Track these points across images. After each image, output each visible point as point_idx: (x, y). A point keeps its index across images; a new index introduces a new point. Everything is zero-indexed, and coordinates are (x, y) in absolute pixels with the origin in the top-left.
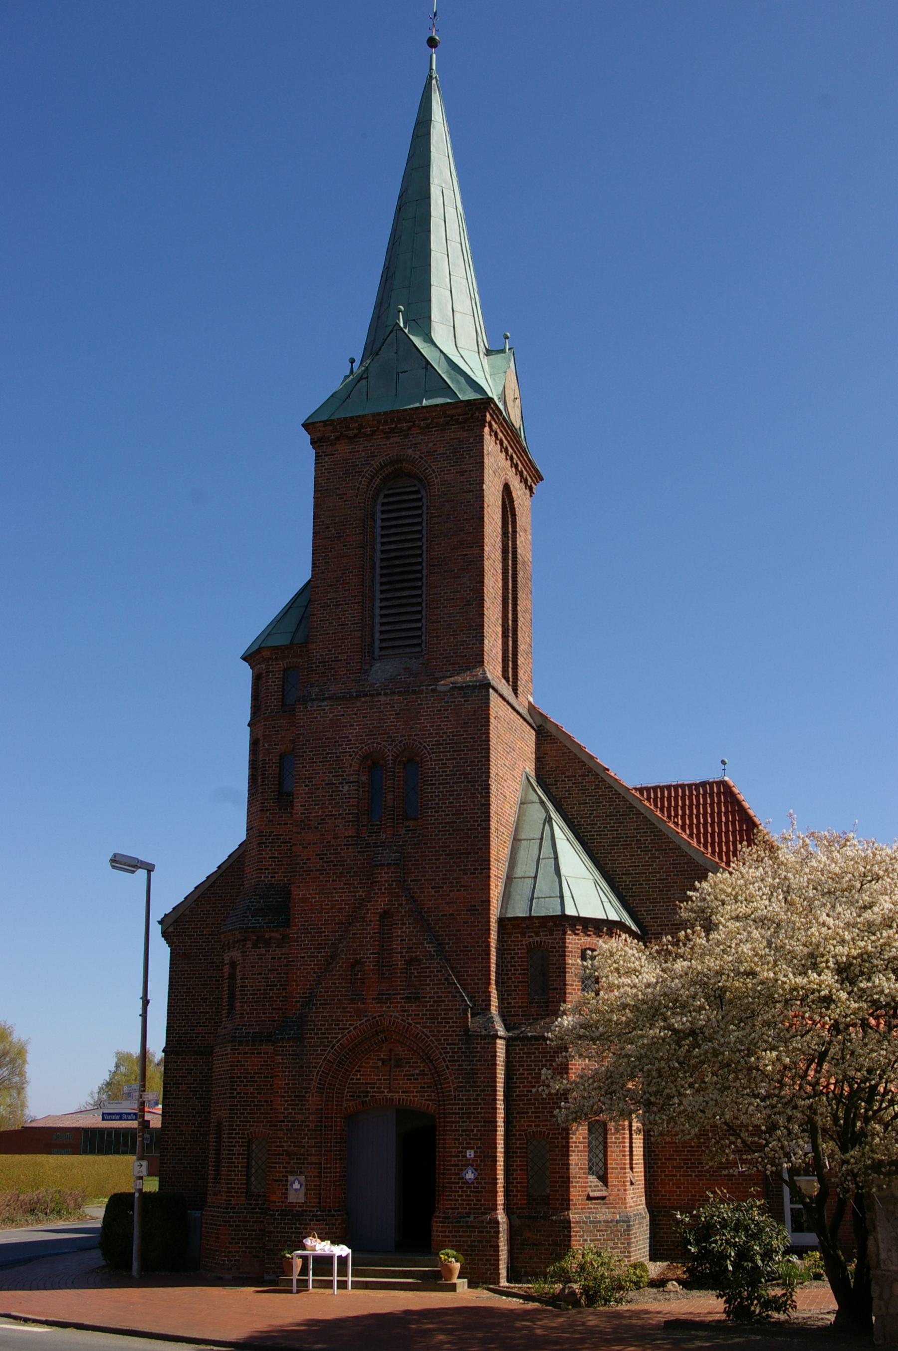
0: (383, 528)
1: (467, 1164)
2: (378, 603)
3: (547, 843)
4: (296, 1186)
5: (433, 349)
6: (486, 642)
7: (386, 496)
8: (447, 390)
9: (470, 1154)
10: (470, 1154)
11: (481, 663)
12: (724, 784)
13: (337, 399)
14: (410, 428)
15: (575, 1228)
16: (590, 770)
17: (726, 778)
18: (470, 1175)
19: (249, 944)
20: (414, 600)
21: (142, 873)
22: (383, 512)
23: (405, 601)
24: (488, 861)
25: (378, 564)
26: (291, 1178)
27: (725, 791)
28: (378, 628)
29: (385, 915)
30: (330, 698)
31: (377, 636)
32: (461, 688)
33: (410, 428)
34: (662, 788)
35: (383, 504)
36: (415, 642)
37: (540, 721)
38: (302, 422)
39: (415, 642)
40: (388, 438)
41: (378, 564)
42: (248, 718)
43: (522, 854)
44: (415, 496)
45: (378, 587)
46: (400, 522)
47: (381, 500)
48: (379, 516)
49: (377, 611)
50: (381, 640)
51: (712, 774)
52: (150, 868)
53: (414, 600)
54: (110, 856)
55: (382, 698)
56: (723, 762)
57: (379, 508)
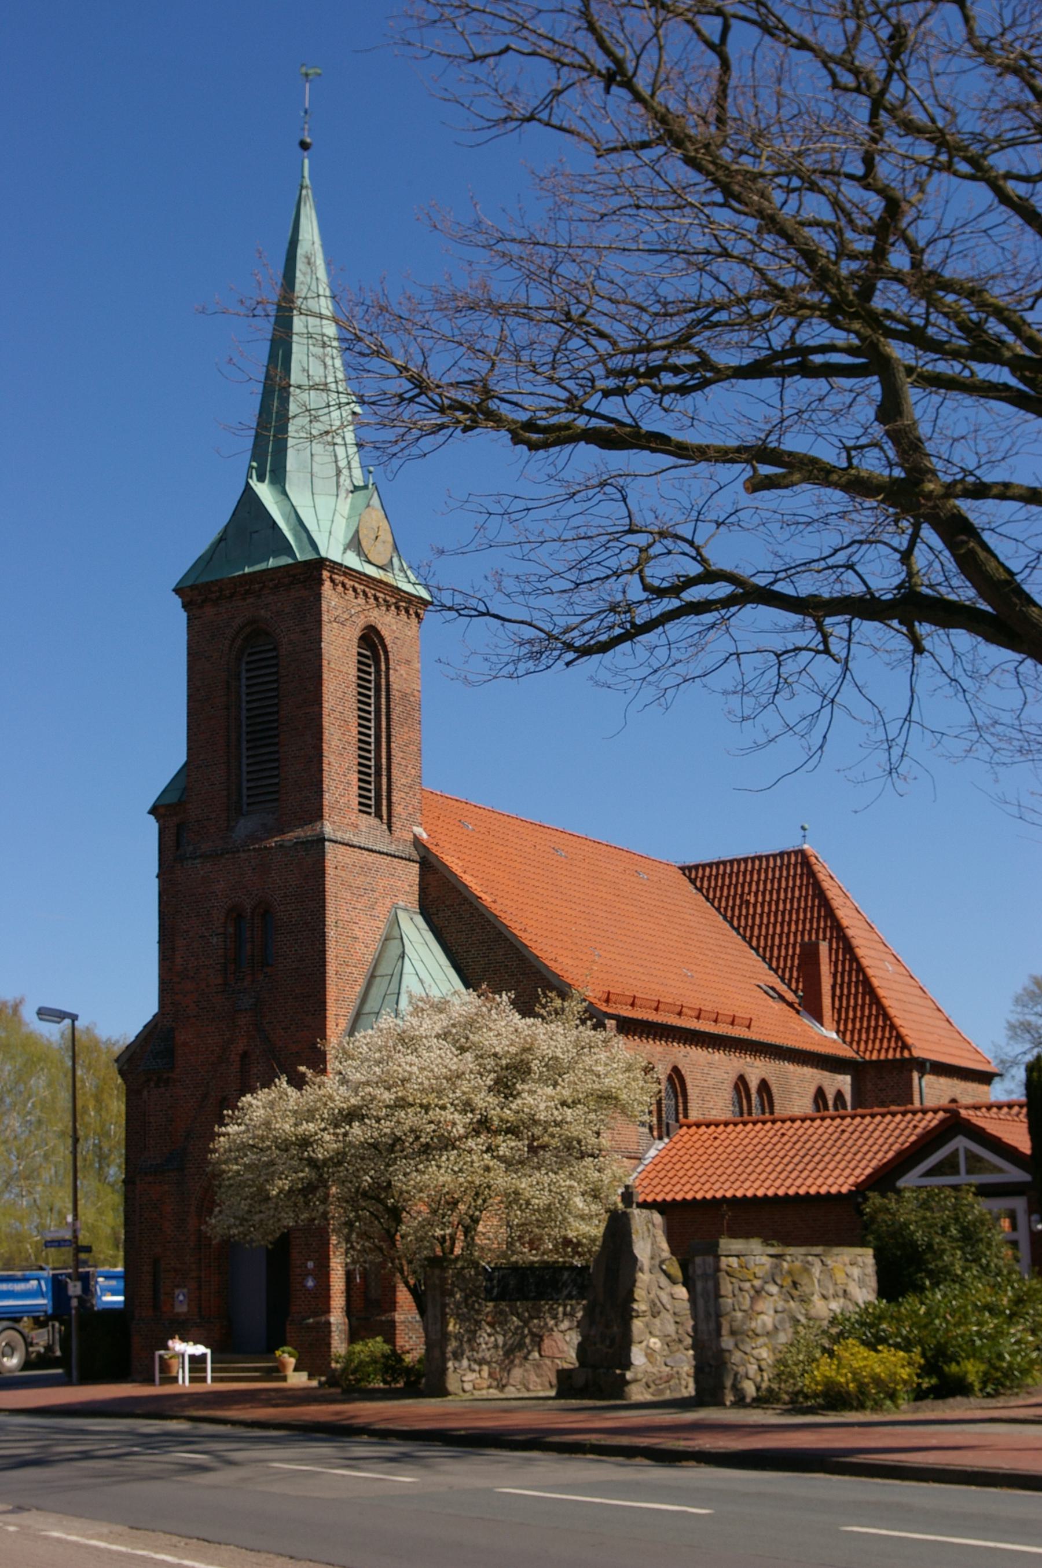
0: (248, 686)
1: (308, 1273)
2: (244, 761)
3: (395, 979)
4: (181, 1298)
5: (286, 502)
6: (326, 796)
7: (250, 655)
8: (288, 550)
9: (310, 1264)
10: (310, 1264)
11: (321, 817)
12: (802, 853)
13: (206, 561)
14: (261, 589)
15: (400, 1328)
16: (466, 899)
17: (806, 847)
18: (310, 1283)
19: (152, 1084)
20: (273, 757)
21: (67, 1022)
22: (248, 671)
23: (265, 758)
24: (324, 1003)
25: (244, 722)
26: (177, 1291)
27: (803, 859)
28: (245, 785)
29: (245, 1055)
30: (201, 856)
31: (245, 792)
32: (303, 843)
33: (261, 589)
34: (739, 861)
35: (247, 663)
36: (275, 796)
37: (423, 853)
38: (173, 586)
39: (275, 796)
40: (244, 599)
41: (244, 722)
42: (156, 870)
43: (374, 990)
44: (270, 655)
45: (244, 745)
46: (260, 680)
47: (245, 659)
48: (244, 675)
49: (244, 768)
50: (248, 796)
51: (789, 845)
52: (74, 1018)
53: (273, 757)
54: (36, 1009)
55: (242, 855)
56: (803, 828)
57: (244, 666)
